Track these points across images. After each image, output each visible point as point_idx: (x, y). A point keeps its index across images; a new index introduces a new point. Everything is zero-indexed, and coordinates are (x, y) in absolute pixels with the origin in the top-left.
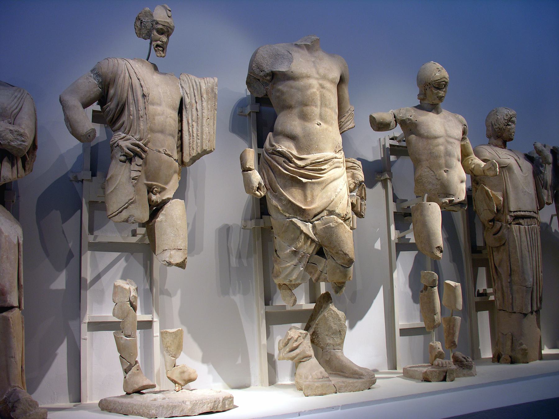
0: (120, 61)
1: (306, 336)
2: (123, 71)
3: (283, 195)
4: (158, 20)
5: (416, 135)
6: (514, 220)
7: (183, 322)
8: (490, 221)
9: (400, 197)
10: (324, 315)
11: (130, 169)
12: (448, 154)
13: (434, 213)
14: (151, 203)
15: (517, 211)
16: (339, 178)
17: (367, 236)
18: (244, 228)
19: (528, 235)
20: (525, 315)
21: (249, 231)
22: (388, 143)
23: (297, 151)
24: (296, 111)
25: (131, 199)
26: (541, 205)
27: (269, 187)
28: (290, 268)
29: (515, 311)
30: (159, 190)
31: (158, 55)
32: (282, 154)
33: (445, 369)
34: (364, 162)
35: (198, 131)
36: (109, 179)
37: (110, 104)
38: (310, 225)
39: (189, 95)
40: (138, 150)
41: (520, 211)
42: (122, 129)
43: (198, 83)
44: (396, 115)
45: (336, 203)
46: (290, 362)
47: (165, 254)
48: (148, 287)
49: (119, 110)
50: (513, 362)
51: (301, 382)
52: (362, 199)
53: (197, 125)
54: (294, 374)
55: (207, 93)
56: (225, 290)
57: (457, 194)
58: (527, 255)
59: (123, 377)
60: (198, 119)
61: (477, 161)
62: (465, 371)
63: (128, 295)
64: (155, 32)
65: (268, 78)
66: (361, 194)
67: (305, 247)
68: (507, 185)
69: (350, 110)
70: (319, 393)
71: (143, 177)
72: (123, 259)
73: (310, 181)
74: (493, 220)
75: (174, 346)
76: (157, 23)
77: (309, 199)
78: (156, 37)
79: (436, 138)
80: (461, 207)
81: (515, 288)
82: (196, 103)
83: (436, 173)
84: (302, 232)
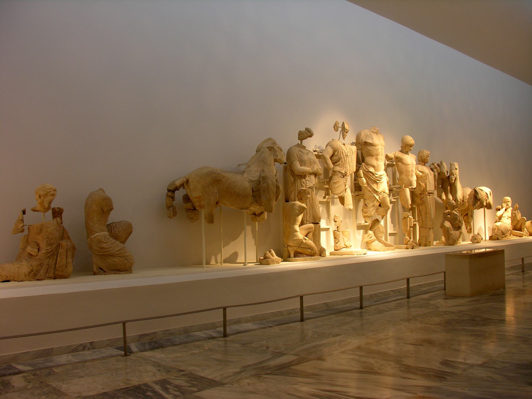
12: (412, 171)
13: (408, 192)
24: (375, 157)
32: (371, 172)
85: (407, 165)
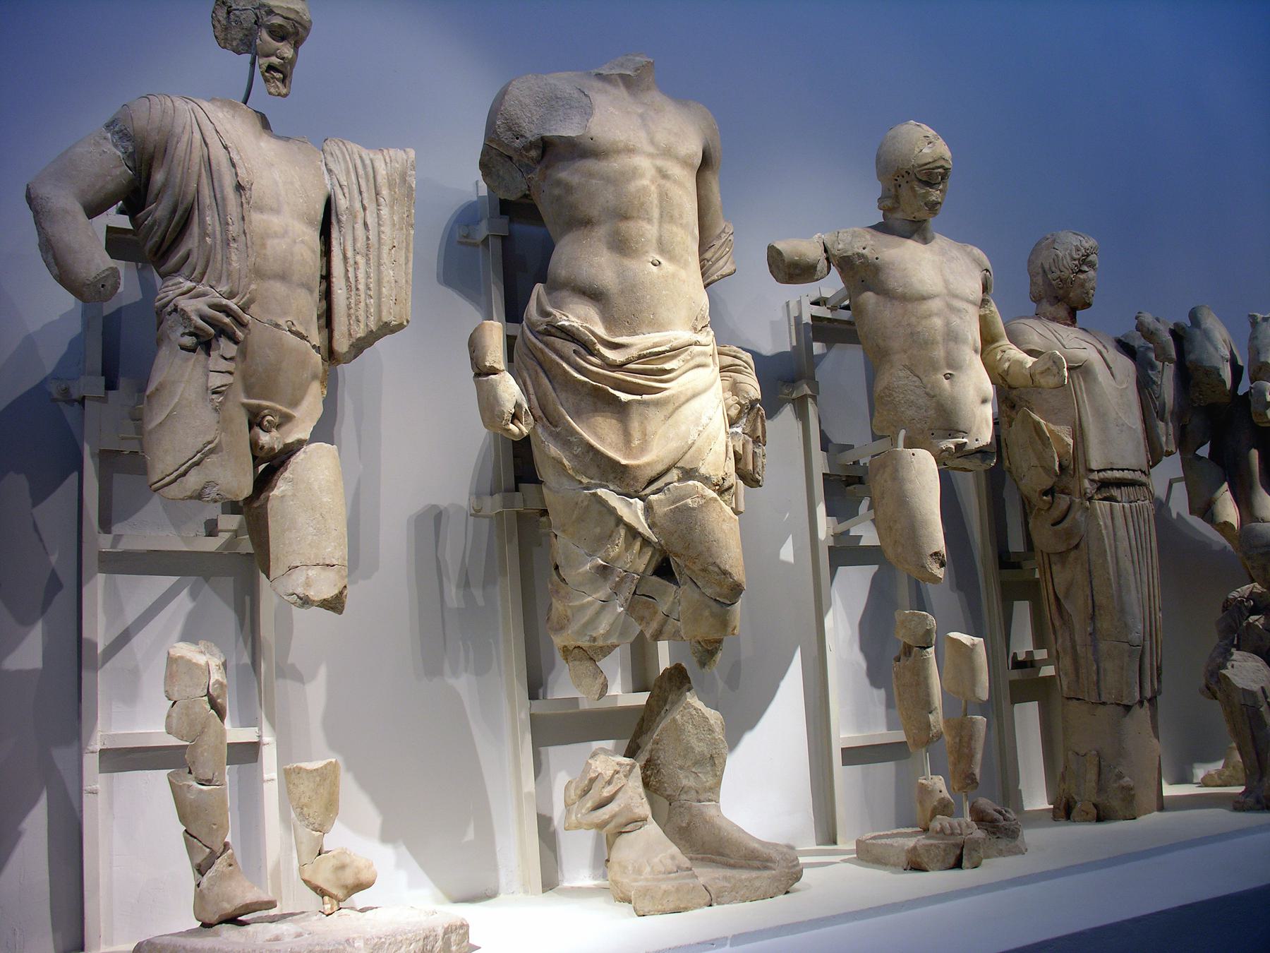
0: (179, 103)
1: (630, 771)
2: (188, 128)
3: (573, 432)
4: (271, 3)
5: (877, 294)
6: (1099, 489)
7: (334, 743)
8: (1045, 493)
9: (837, 438)
10: (674, 720)
11: (206, 367)
12: (953, 336)
13: (924, 472)
14: (260, 454)
15: (1104, 470)
16: (704, 391)
17: (765, 531)
18: (477, 513)
19: (1131, 524)
20: (1128, 708)
21: (487, 521)
22: (808, 312)
23: (606, 328)
24: (601, 231)
25: (209, 443)
26: (1155, 454)
27: (539, 413)
28: (593, 610)
29: (1103, 700)
30: (277, 420)
31: (272, 90)
32: (569, 334)
33: (959, 839)
34: (756, 356)
35: (368, 277)
36: (153, 394)
37: (154, 210)
38: (639, 504)
39: (346, 190)
40: (227, 320)
41: (1112, 469)
42: (186, 270)
43: (368, 162)
44: (829, 246)
45: (700, 451)
46: (592, 832)
47: (294, 577)
48: (246, 659)
49: (178, 223)
50: (1101, 816)
51: (626, 881)
52: (756, 441)
53: (368, 263)
54: (603, 862)
55: (391, 186)
56: (432, 667)
57: (974, 429)
58: (1131, 570)
59: (193, 884)
60: (368, 247)
61: (1016, 353)
62: (1003, 843)
63: (205, 680)
64: (264, 35)
65: (533, 153)
66: (754, 430)
67: (629, 557)
68: (1082, 410)
69: (723, 231)
70: (672, 906)
71: (239, 387)
72: (185, 592)
73: (638, 397)
74: (1050, 492)
75: (316, 805)
76: (270, 12)
77: (636, 443)
78: (265, 46)
79: (924, 298)
80: (983, 460)
81: (1103, 646)
82: (364, 209)
83: (925, 380)
84: (619, 520)
85: (910, 298)
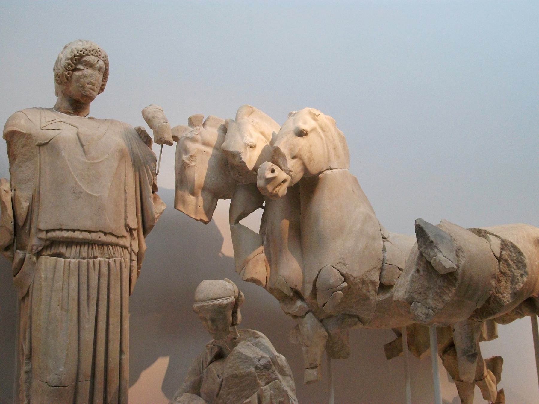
15: (54, 230)
41: (61, 230)
81: (35, 383)
